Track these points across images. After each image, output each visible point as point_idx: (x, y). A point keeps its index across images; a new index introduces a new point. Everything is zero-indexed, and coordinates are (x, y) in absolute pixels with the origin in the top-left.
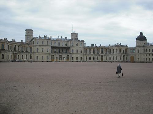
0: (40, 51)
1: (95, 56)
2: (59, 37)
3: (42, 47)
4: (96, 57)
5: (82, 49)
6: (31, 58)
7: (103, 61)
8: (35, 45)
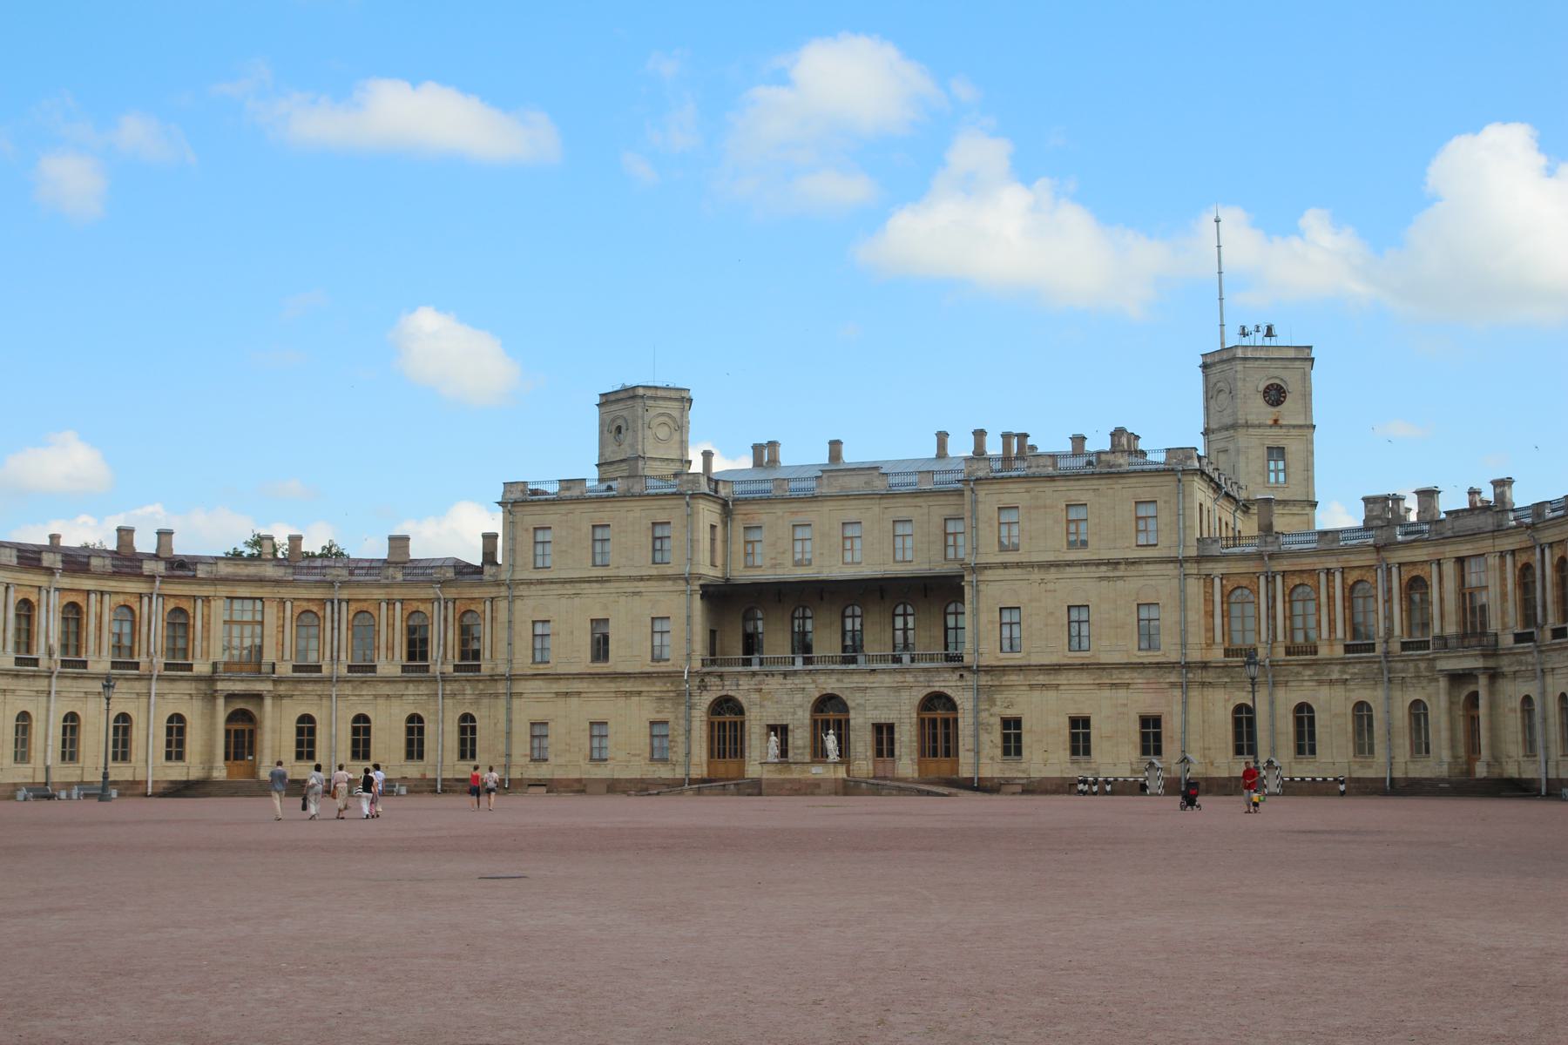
0: (573, 652)
1: (1374, 696)
2: (942, 437)
3: (593, 604)
4: (1392, 707)
5: (1161, 584)
6: (467, 749)
7: (1481, 771)
8: (512, 584)
